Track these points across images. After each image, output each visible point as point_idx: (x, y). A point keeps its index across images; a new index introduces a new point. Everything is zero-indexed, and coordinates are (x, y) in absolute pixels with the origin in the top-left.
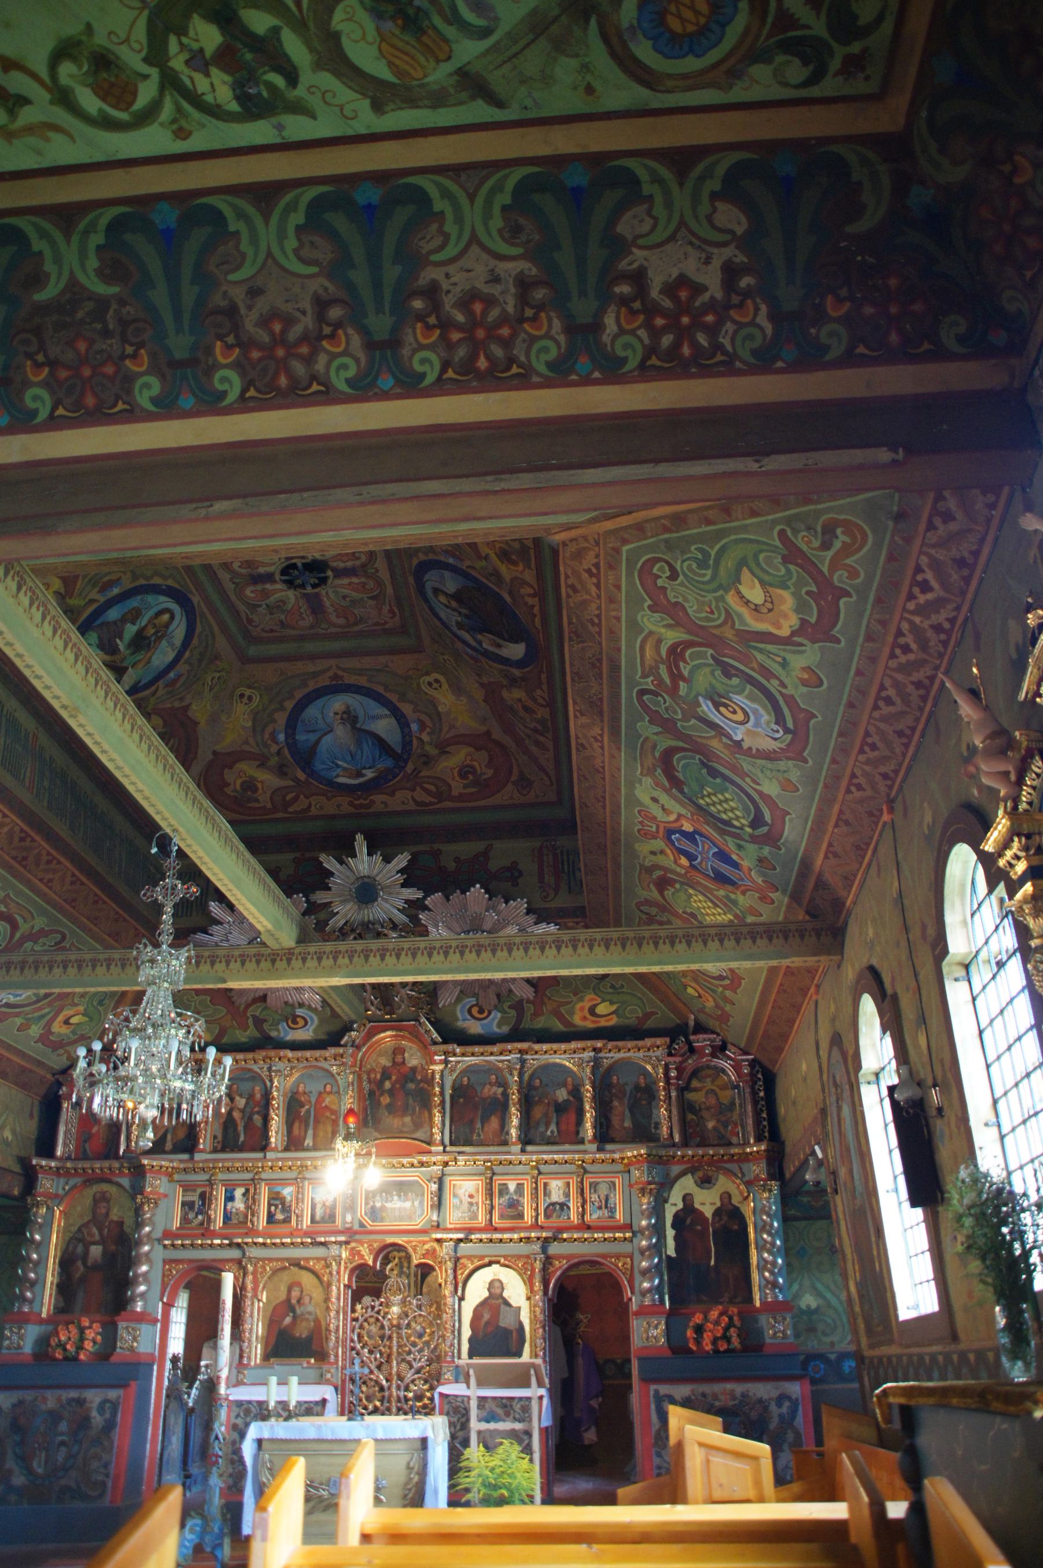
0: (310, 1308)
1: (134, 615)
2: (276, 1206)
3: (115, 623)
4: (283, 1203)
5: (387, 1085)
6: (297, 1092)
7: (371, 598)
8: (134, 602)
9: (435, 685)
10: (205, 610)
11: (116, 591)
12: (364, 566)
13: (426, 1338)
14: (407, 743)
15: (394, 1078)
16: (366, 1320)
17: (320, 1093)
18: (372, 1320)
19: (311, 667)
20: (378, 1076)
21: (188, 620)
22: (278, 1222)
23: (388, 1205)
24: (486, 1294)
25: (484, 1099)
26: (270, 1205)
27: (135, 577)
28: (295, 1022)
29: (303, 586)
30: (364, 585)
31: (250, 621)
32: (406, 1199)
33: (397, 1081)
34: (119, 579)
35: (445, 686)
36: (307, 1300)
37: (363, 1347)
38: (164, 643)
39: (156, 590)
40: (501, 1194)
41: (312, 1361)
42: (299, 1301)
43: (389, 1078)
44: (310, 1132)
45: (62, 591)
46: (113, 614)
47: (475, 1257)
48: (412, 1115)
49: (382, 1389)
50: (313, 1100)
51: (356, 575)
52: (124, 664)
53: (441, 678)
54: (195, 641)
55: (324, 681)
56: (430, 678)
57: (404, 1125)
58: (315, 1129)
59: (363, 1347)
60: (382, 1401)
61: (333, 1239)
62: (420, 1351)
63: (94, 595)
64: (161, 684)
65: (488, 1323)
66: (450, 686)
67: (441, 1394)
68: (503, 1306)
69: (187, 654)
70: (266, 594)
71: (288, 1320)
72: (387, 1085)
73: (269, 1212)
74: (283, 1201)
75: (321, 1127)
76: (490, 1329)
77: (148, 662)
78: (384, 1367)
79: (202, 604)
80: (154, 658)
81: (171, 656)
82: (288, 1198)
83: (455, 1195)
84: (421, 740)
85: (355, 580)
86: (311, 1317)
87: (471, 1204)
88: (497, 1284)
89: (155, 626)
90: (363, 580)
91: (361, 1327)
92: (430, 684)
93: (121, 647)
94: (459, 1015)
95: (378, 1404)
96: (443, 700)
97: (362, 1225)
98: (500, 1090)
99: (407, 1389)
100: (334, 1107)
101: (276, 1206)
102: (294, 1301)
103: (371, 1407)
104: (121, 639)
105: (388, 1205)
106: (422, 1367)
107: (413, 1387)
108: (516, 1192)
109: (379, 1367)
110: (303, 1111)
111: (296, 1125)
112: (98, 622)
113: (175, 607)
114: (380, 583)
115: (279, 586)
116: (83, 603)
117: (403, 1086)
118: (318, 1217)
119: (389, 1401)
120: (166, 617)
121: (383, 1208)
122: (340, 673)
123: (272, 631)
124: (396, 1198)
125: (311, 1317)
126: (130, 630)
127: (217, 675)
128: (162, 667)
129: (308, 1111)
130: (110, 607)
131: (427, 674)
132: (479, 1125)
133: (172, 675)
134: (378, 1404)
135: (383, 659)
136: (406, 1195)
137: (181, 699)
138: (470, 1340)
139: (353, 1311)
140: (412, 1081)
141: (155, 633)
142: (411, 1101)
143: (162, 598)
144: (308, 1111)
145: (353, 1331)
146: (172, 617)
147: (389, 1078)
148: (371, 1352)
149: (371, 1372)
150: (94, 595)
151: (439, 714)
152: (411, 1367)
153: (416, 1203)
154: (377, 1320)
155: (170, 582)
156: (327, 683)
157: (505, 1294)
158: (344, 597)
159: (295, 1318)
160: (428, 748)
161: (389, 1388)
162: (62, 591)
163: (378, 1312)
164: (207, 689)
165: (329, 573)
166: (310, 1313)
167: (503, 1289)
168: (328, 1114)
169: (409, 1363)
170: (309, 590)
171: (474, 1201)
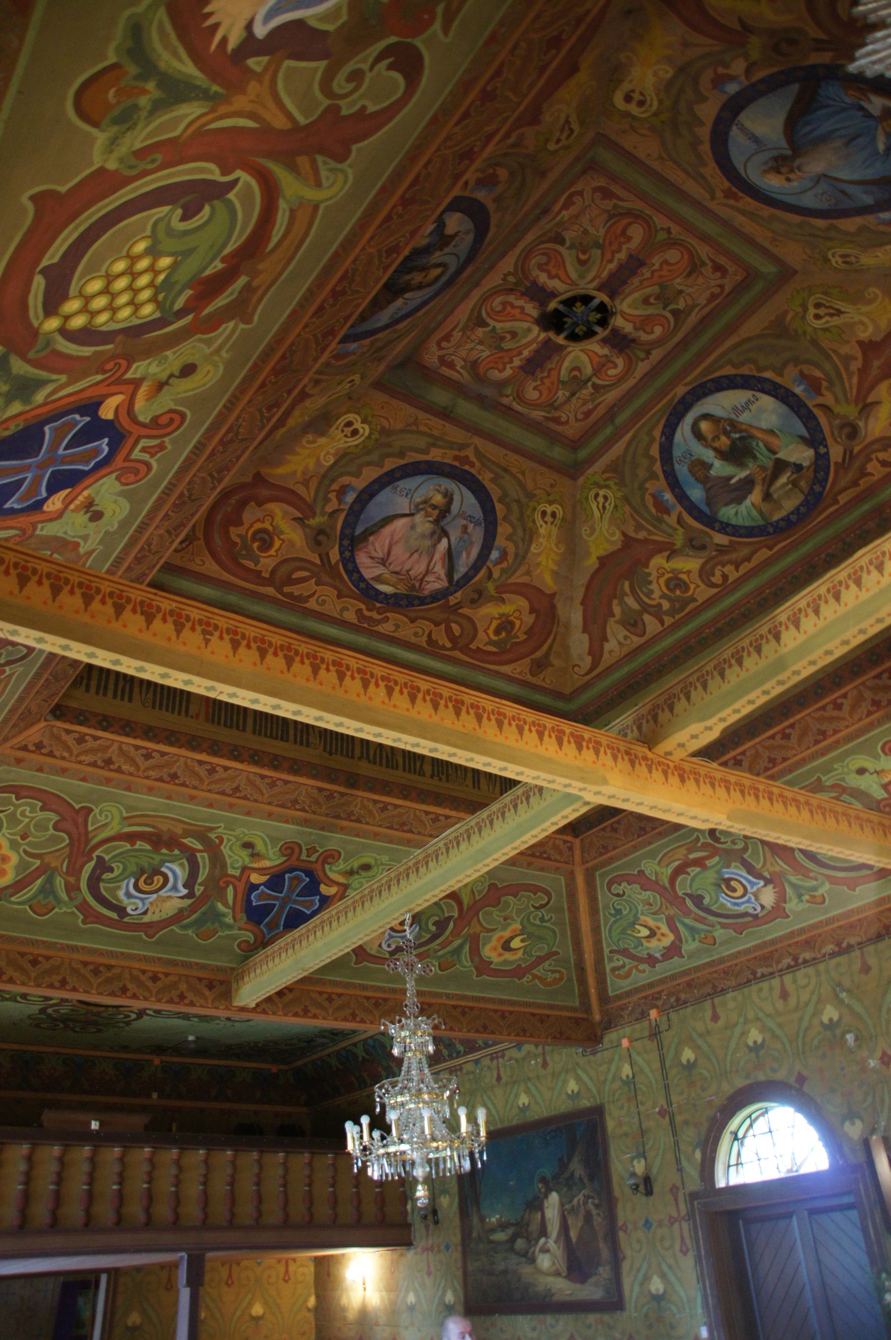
1: (700, 468)
3: (707, 491)
7: (562, 242)
8: (682, 470)
9: (636, 97)
10: (699, 370)
11: (668, 496)
12: (511, 291)
14: (770, 86)
19: (739, 220)
21: (711, 392)
27: (653, 476)
29: (602, 308)
30: (540, 267)
31: (713, 297)
34: (653, 495)
35: (626, 87)
38: (744, 418)
39: (667, 450)
45: (667, 553)
46: (696, 494)
51: (534, 283)
52: (770, 464)
53: (618, 99)
54: (745, 370)
55: (748, 203)
56: (633, 109)
63: (672, 520)
64: (810, 404)
66: (620, 81)
69: (768, 375)
70: (644, 323)
77: (771, 432)
79: (689, 379)
80: (764, 425)
81: (767, 401)
84: (748, 72)
85: (543, 278)
89: (716, 438)
90: (535, 273)
92: (641, 104)
93: (743, 474)
96: (649, 82)
104: (732, 477)
112: (706, 509)
113: (689, 418)
114: (527, 255)
115: (618, 322)
116: (681, 531)
120: (704, 426)
122: (719, 194)
123: (717, 268)
126: (720, 468)
127: (812, 311)
128: (784, 409)
130: (687, 498)
131: (628, 114)
133: (798, 390)
135: (656, 165)
137: (847, 359)
141: (726, 433)
143: (678, 437)
146: (706, 417)
150: (672, 520)
151: (682, 70)
155: (657, 433)
156: (748, 199)
158: (582, 263)
160: (755, 54)
162: (667, 553)
164: (836, 321)
165: (552, 305)
170: (602, 297)
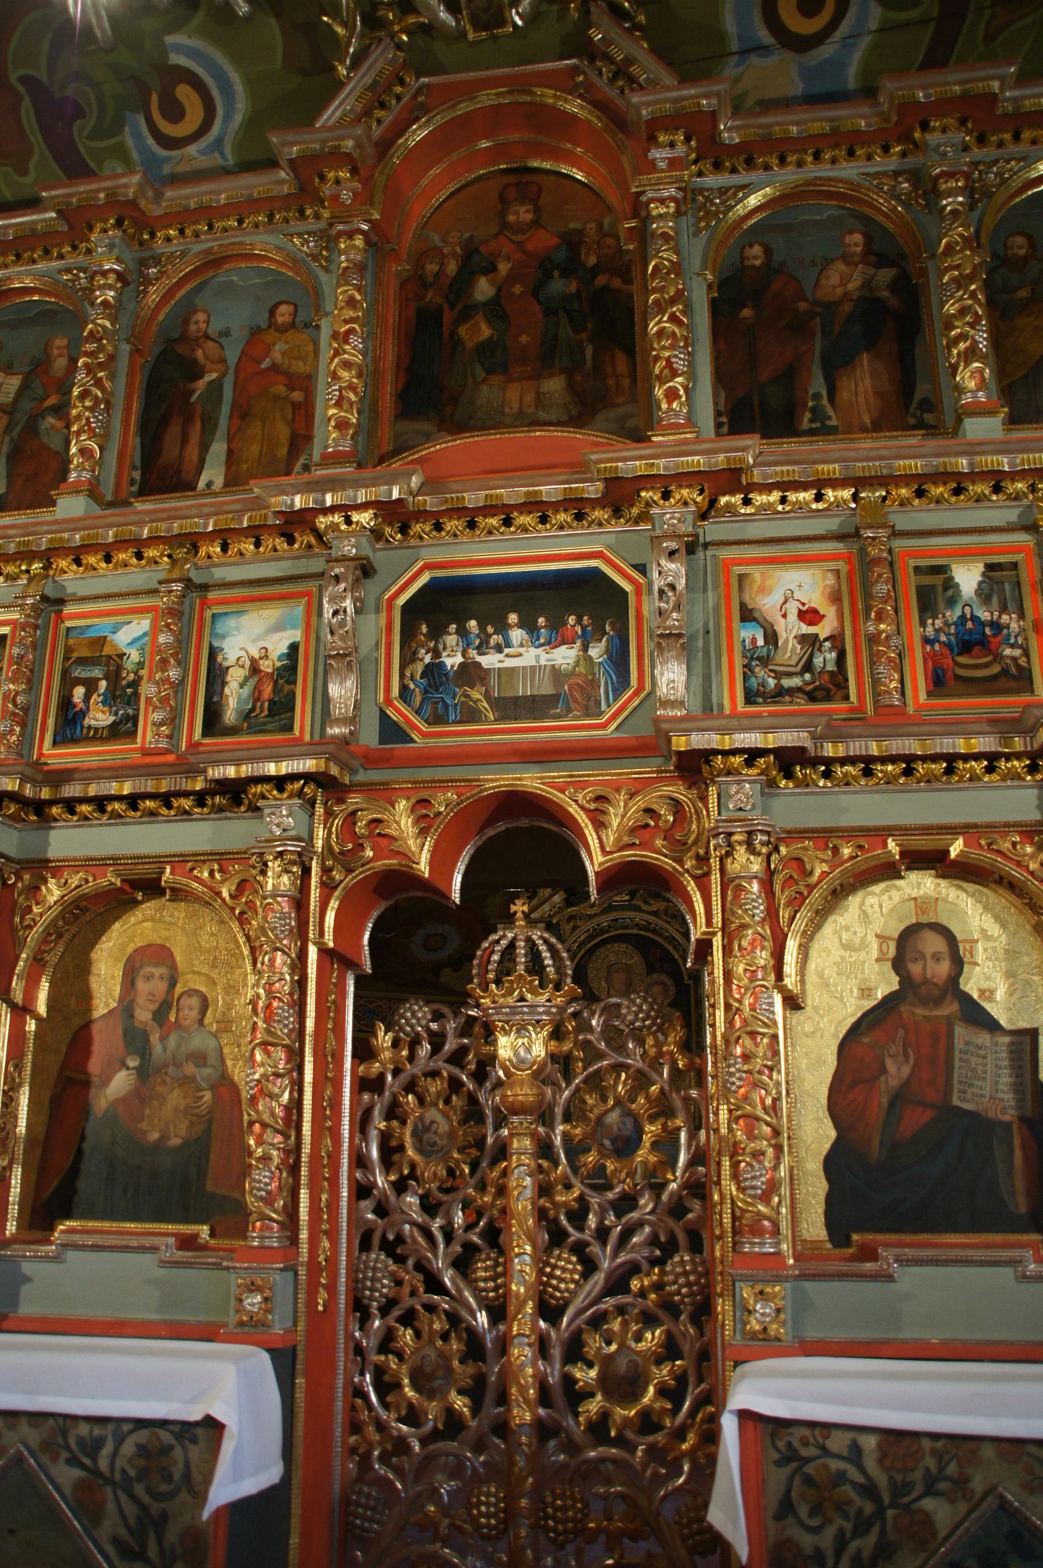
0: (198, 1041)
2: (91, 685)
4: (114, 676)
5: (484, 289)
6: (184, 338)
13: (644, 1154)
15: (503, 268)
16: (410, 1087)
17: (256, 333)
18: (434, 1087)
20: (452, 268)
22: (97, 736)
23: (489, 661)
24: (886, 984)
25: (829, 307)
26: (68, 682)
28: (175, 112)
32: (559, 638)
33: (512, 278)
36: (190, 1008)
37: (400, 1187)
40: (927, 604)
41: (204, 1231)
42: (160, 1015)
43: (490, 269)
44: (219, 448)
47: (849, 833)
48: (569, 373)
49: (474, 1344)
50: (232, 355)
57: (540, 401)
58: (230, 438)
59: (400, 1187)
60: (476, 1392)
61: (271, 769)
62: (626, 1203)
65: (899, 1098)
67: (745, 1416)
68: (960, 1031)
71: (121, 1083)
72: (484, 289)
73: (66, 703)
74: (114, 664)
75: (255, 428)
76: (916, 1118)
78: (481, 1269)
82: (135, 656)
83: (747, 615)
86: (204, 1074)
87: (810, 642)
88: (933, 943)
91: (393, 1112)
94: (730, 24)
95: (460, 1403)
97: (391, 731)
98: (885, 275)
99: (574, 1352)
100: (299, 367)
101: (91, 685)
102: (143, 1015)
103: (433, 1410)
105: (489, 661)
106: (633, 1269)
107: (594, 1343)
108: (984, 594)
109: (463, 1264)
110: (201, 384)
111: (173, 432)
117: (536, 291)
118: (230, 715)
119: (503, 1399)
121: (470, 673)
124: (517, 635)
125: (204, 1074)
129: (216, 387)
132: (817, 384)
134: (460, 1403)
136: (556, 625)
138: (832, 1164)
139: (364, 1051)
140: (565, 274)
142: (565, 331)
144: (216, 387)
145: (362, 1123)
147: (490, 269)
148: (429, 1207)
149: (434, 1284)
152: (589, 1267)
153: (596, 651)
154: (455, 1084)
157: (971, 985)
159: (143, 1073)
161: (503, 1345)
163: (457, 1058)
166: (200, 1058)
167: (958, 963)
168: (280, 389)
169: (579, 1249)
171: (823, 630)
